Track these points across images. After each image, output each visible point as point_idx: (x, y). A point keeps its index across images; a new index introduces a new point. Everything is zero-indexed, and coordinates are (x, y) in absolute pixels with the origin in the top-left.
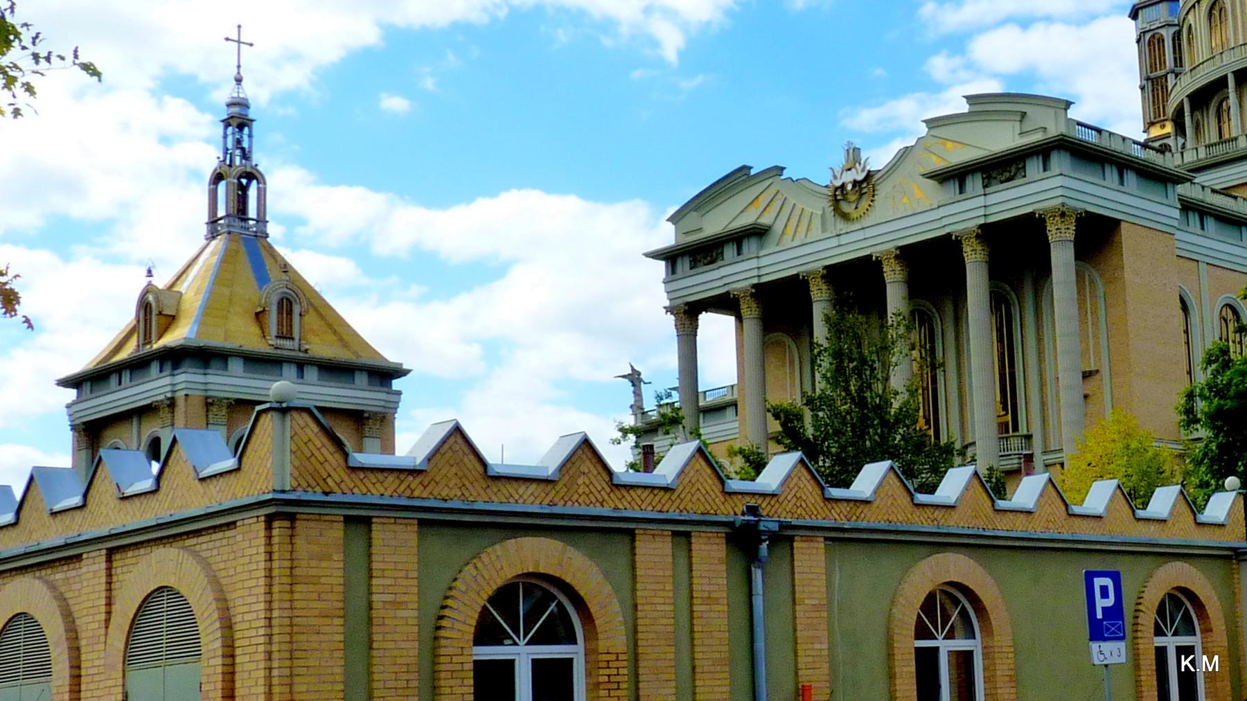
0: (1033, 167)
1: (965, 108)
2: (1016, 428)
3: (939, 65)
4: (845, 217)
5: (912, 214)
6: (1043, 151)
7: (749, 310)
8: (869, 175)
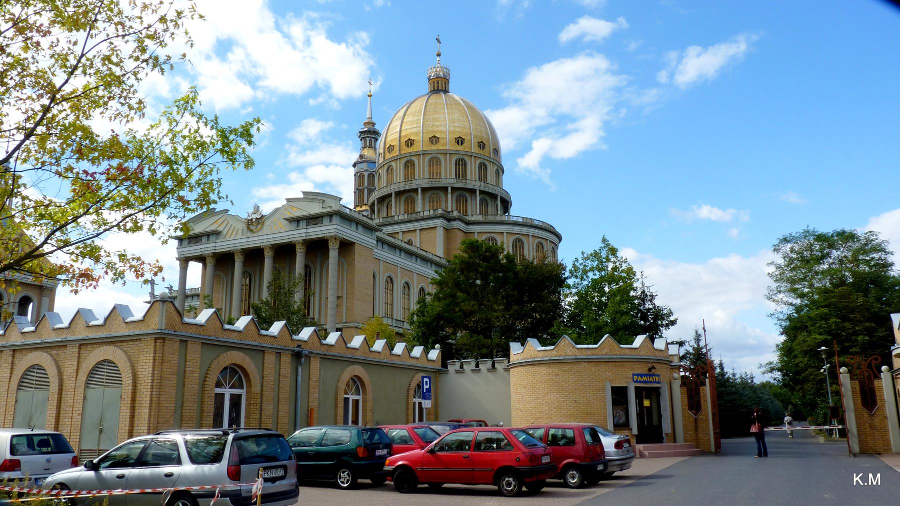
0: (326, 220)
1: (302, 196)
2: (308, 315)
3: (293, 176)
4: (251, 231)
5: (277, 233)
6: (330, 215)
7: (210, 262)
8: (262, 216)
